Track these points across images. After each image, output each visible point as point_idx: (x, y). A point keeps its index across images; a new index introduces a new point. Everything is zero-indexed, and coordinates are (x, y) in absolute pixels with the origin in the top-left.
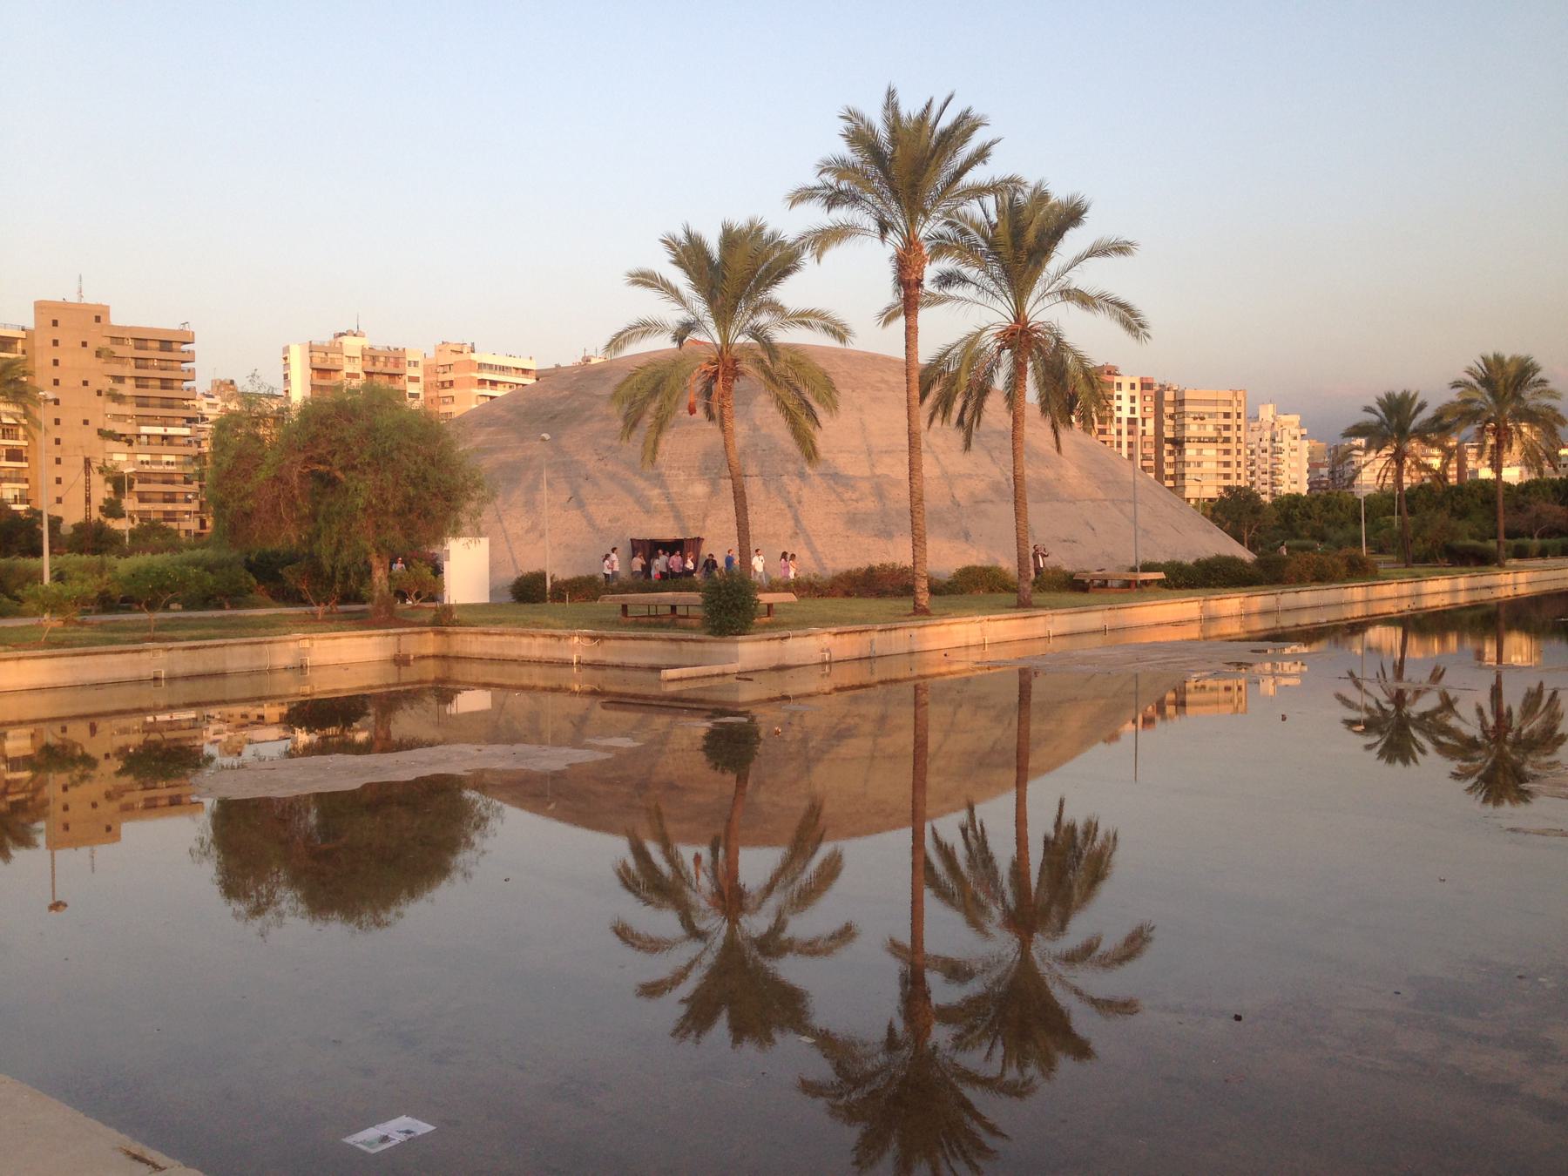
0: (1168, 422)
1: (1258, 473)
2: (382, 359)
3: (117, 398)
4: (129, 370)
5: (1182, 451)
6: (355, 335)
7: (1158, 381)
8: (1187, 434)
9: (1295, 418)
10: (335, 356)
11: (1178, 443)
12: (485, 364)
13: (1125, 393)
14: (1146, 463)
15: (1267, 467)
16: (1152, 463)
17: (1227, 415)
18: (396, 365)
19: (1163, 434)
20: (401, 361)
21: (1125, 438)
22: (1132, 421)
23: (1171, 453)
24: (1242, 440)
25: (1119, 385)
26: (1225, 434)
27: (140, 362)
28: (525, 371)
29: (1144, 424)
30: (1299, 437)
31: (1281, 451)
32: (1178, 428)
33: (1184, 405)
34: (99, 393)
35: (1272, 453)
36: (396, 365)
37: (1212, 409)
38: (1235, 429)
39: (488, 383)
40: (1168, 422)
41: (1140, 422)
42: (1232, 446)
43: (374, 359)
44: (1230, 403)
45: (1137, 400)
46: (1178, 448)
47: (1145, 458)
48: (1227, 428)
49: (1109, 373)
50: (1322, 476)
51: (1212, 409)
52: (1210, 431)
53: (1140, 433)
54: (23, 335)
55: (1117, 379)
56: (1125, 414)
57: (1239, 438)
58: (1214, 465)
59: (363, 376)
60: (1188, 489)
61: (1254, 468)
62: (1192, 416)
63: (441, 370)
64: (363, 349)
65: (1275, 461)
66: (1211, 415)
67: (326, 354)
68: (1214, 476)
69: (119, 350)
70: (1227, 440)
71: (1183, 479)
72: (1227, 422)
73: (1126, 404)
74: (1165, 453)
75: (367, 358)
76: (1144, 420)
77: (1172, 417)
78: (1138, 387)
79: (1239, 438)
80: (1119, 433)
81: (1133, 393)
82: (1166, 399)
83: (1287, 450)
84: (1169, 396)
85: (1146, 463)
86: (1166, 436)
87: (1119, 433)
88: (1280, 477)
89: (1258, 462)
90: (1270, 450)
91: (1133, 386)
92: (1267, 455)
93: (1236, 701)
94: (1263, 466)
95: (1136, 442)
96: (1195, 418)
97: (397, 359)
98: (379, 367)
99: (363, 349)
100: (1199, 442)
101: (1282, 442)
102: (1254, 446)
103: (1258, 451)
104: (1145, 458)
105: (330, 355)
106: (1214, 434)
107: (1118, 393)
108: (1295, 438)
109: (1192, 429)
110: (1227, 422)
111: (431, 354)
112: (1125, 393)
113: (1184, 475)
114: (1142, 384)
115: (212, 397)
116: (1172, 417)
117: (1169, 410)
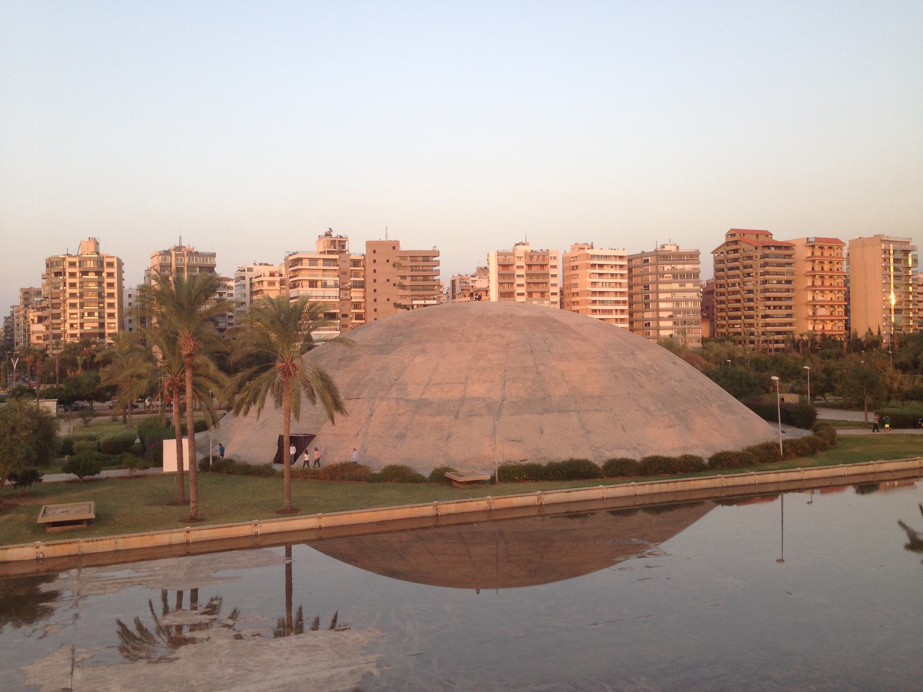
2: (536, 257)
3: (403, 287)
4: (408, 273)
6: (524, 244)
10: (510, 257)
12: (594, 255)
18: (543, 260)
20: (546, 257)
27: (414, 268)
28: (621, 257)
34: (394, 285)
36: (543, 260)
39: (597, 266)
43: (531, 257)
54: (363, 258)
59: (525, 267)
63: (572, 259)
64: (526, 252)
67: (506, 257)
69: (403, 263)
75: (528, 257)
97: (544, 256)
98: (534, 261)
99: (526, 252)
111: (569, 251)
115: (475, 277)
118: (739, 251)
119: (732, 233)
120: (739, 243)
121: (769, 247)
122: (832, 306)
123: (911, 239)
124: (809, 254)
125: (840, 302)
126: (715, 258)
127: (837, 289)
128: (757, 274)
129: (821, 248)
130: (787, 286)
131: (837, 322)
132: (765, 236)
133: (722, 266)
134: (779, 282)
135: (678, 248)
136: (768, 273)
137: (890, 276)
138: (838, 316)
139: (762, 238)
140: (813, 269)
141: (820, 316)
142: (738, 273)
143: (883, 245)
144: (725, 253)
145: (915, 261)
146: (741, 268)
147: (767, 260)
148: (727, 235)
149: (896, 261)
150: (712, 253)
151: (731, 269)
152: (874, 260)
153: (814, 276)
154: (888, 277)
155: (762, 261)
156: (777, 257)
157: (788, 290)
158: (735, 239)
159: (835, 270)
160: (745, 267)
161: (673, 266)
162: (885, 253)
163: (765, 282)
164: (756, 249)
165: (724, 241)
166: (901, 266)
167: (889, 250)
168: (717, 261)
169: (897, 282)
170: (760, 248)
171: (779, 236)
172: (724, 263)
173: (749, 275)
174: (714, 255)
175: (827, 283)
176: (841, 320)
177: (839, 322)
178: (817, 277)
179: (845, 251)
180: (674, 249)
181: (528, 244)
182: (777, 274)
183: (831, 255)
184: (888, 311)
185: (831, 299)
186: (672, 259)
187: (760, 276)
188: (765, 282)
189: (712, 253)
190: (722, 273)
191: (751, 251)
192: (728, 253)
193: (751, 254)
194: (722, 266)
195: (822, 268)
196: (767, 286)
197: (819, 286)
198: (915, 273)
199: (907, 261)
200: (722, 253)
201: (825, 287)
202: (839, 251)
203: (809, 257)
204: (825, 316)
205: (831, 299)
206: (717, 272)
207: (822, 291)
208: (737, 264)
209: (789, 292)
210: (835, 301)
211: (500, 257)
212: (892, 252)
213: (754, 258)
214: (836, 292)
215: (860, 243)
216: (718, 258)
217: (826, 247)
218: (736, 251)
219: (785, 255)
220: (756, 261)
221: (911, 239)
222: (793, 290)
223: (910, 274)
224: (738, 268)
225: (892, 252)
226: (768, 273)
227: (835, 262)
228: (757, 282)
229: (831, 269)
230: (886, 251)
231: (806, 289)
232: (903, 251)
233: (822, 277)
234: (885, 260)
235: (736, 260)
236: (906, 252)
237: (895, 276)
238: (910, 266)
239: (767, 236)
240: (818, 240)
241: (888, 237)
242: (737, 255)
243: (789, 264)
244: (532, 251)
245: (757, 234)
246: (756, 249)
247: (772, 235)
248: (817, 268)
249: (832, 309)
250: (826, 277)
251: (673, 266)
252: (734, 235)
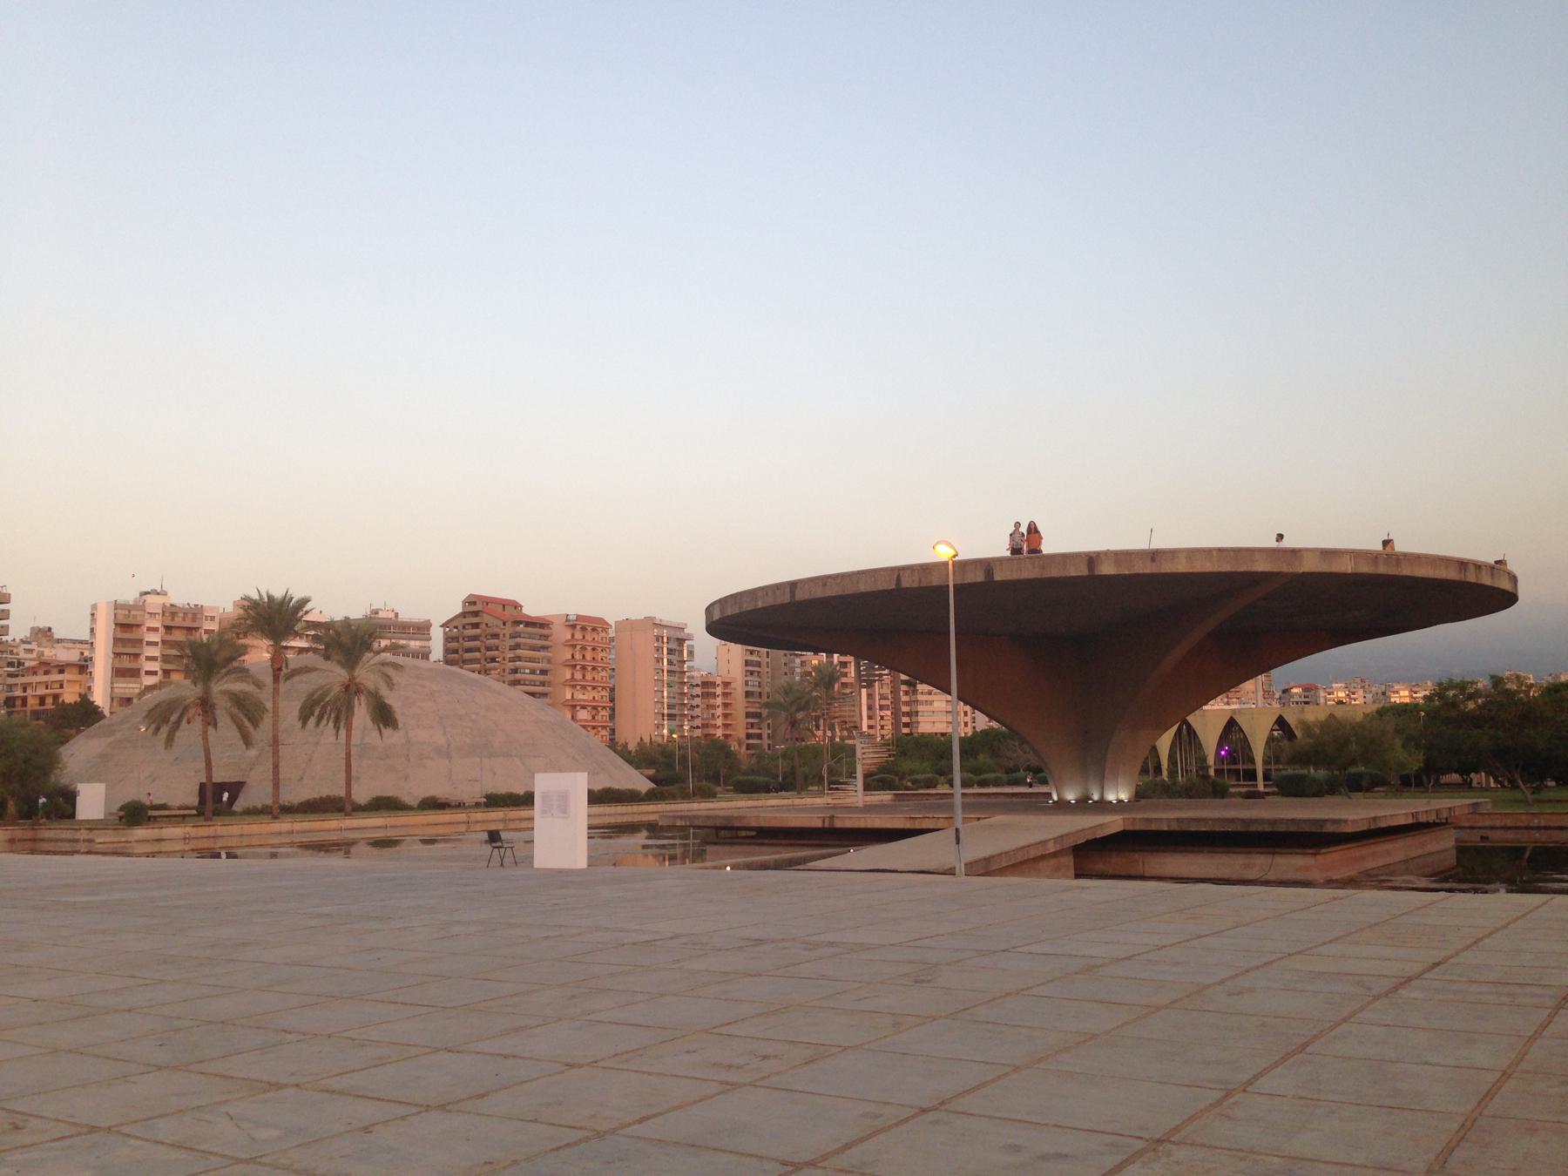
2: (181, 615)
5: (915, 692)
6: (158, 594)
14: (883, 702)
18: (194, 619)
20: (199, 616)
23: (906, 693)
36: (194, 619)
43: (173, 615)
46: (912, 688)
47: (882, 697)
58: (944, 704)
59: (162, 630)
60: (921, 725)
67: (129, 611)
74: (902, 693)
85: (883, 702)
97: (195, 614)
98: (178, 622)
104: (882, 697)
105: (132, 613)
113: (917, 712)
118: (481, 626)
119: (471, 601)
120: (480, 614)
121: (517, 623)
122: (595, 708)
123: (686, 625)
124: (569, 637)
125: (604, 702)
126: (445, 633)
127: (602, 685)
128: (504, 659)
129: (584, 629)
130: (542, 678)
131: (600, 729)
132: (513, 608)
133: (454, 645)
134: (533, 672)
135: (397, 615)
136: (519, 658)
137: (663, 671)
138: (601, 722)
139: (509, 611)
140: (573, 657)
141: (581, 720)
142: (479, 657)
143: (655, 630)
144: (460, 628)
145: (691, 653)
146: (483, 650)
147: (519, 640)
148: (464, 602)
149: (670, 651)
150: (441, 626)
151: (468, 650)
152: (645, 647)
153: (574, 666)
154: (660, 671)
155: (512, 642)
156: (531, 636)
157: (543, 684)
158: (476, 608)
159: (599, 659)
160: (489, 649)
161: (393, 641)
162: (658, 640)
163: (515, 671)
164: (504, 624)
165: (459, 610)
166: (674, 658)
167: (663, 637)
168: (448, 639)
169: (672, 678)
170: (509, 625)
171: (531, 610)
172: (458, 642)
173: (493, 660)
174: (444, 630)
175: (589, 677)
176: (604, 727)
177: (602, 729)
178: (578, 667)
179: (612, 633)
180: (392, 615)
181: (165, 594)
182: (531, 660)
183: (594, 639)
184: (661, 716)
185: (594, 698)
186: (392, 630)
187: (510, 661)
188: (515, 671)
189: (441, 626)
190: (478, 654)
191: (497, 626)
192: (464, 627)
193: (497, 630)
194: (454, 645)
195: (584, 656)
196: (518, 676)
197: (580, 680)
198: (691, 669)
199: (681, 652)
200: (456, 627)
201: (587, 681)
202: (603, 634)
203: (567, 641)
204: (586, 721)
205: (594, 698)
206: (448, 654)
207: (584, 687)
208: (477, 643)
209: (544, 686)
210: (597, 701)
211: (119, 611)
212: (665, 640)
213: (501, 636)
214: (600, 689)
215: (627, 625)
216: (450, 634)
217: (589, 628)
218: (476, 626)
219: (541, 636)
220: (503, 641)
221: (686, 625)
222: (550, 684)
223: (686, 670)
224: (478, 650)
225: (665, 640)
226: (519, 658)
227: (600, 649)
228: (504, 670)
229: (594, 659)
230: (659, 638)
231: (564, 684)
232: (678, 639)
233: (584, 668)
234: (658, 650)
235: (475, 638)
236: (681, 641)
237: (668, 671)
238: (685, 659)
239: (515, 607)
240: (579, 617)
241: (661, 620)
242: (477, 631)
243: (545, 648)
244: (172, 605)
245: (504, 604)
246: (504, 624)
247: (521, 607)
248: (578, 656)
249: (594, 713)
250: (589, 668)
251: (393, 641)
252: (474, 603)
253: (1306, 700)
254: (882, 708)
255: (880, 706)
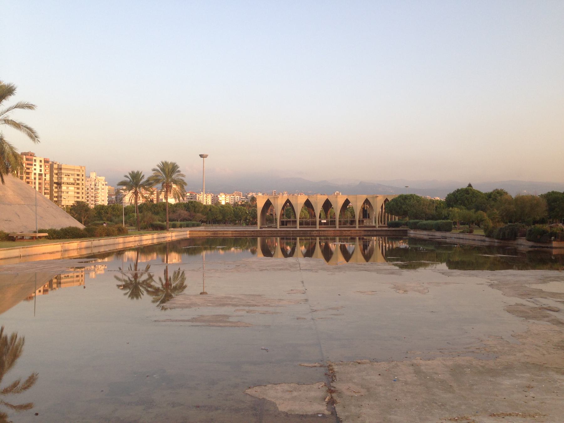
0: (55, 176)
1: (90, 197)
5: (60, 187)
7: (51, 160)
8: (63, 181)
9: (103, 178)
11: (59, 184)
13: (38, 163)
14: (46, 191)
15: (93, 195)
16: (48, 191)
17: (78, 175)
19: (53, 180)
21: (37, 181)
22: (40, 175)
23: (56, 188)
24: (84, 184)
25: (35, 161)
26: (78, 182)
29: (45, 176)
30: (105, 185)
31: (98, 189)
32: (59, 179)
33: (61, 170)
35: (95, 190)
37: (72, 172)
38: (81, 180)
40: (55, 176)
41: (44, 175)
42: (80, 186)
44: (79, 171)
45: (43, 167)
47: (46, 189)
48: (78, 180)
49: (31, 155)
50: (113, 199)
51: (72, 172)
52: (72, 180)
53: (44, 180)
55: (34, 158)
56: (38, 172)
57: (83, 184)
58: (73, 193)
61: (88, 195)
62: (65, 174)
65: (96, 193)
66: (72, 175)
68: (73, 197)
70: (78, 184)
71: (61, 198)
72: (78, 177)
73: (38, 168)
74: (54, 188)
76: (45, 174)
77: (57, 174)
78: (43, 162)
79: (83, 184)
80: (35, 179)
81: (41, 164)
82: (54, 167)
83: (100, 189)
84: (55, 166)
85: (46, 191)
86: (54, 181)
87: (35, 179)
88: (98, 199)
89: (90, 193)
90: (94, 189)
91: (41, 161)
92: (93, 191)
93: (80, 281)
94: (91, 194)
95: (42, 183)
96: (66, 175)
100: (68, 184)
101: (98, 186)
102: (88, 187)
103: (90, 189)
104: (46, 189)
106: (73, 182)
107: (35, 163)
108: (103, 185)
109: (65, 179)
110: (78, 177)
112: (38, 163)
114: (45, 161)
116: (57, 174)
117: (56, 171)
253: (191, 198)
254: (45, 193)
255: (44, 192)
